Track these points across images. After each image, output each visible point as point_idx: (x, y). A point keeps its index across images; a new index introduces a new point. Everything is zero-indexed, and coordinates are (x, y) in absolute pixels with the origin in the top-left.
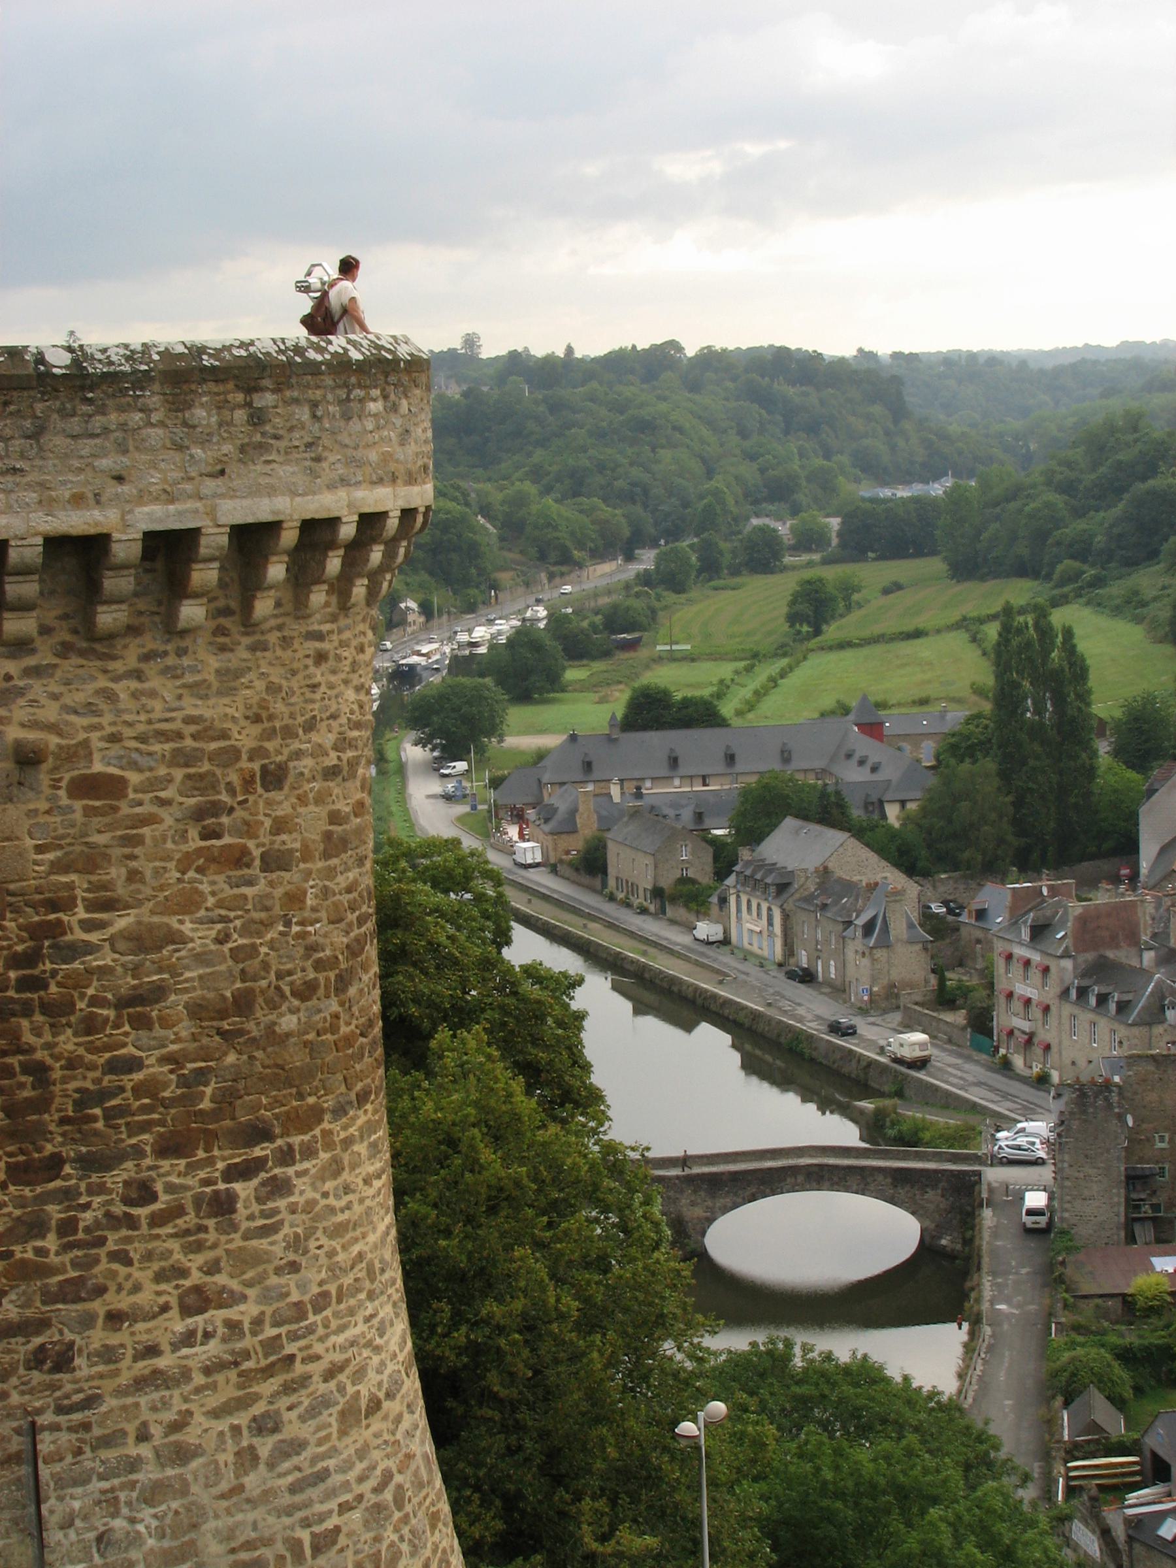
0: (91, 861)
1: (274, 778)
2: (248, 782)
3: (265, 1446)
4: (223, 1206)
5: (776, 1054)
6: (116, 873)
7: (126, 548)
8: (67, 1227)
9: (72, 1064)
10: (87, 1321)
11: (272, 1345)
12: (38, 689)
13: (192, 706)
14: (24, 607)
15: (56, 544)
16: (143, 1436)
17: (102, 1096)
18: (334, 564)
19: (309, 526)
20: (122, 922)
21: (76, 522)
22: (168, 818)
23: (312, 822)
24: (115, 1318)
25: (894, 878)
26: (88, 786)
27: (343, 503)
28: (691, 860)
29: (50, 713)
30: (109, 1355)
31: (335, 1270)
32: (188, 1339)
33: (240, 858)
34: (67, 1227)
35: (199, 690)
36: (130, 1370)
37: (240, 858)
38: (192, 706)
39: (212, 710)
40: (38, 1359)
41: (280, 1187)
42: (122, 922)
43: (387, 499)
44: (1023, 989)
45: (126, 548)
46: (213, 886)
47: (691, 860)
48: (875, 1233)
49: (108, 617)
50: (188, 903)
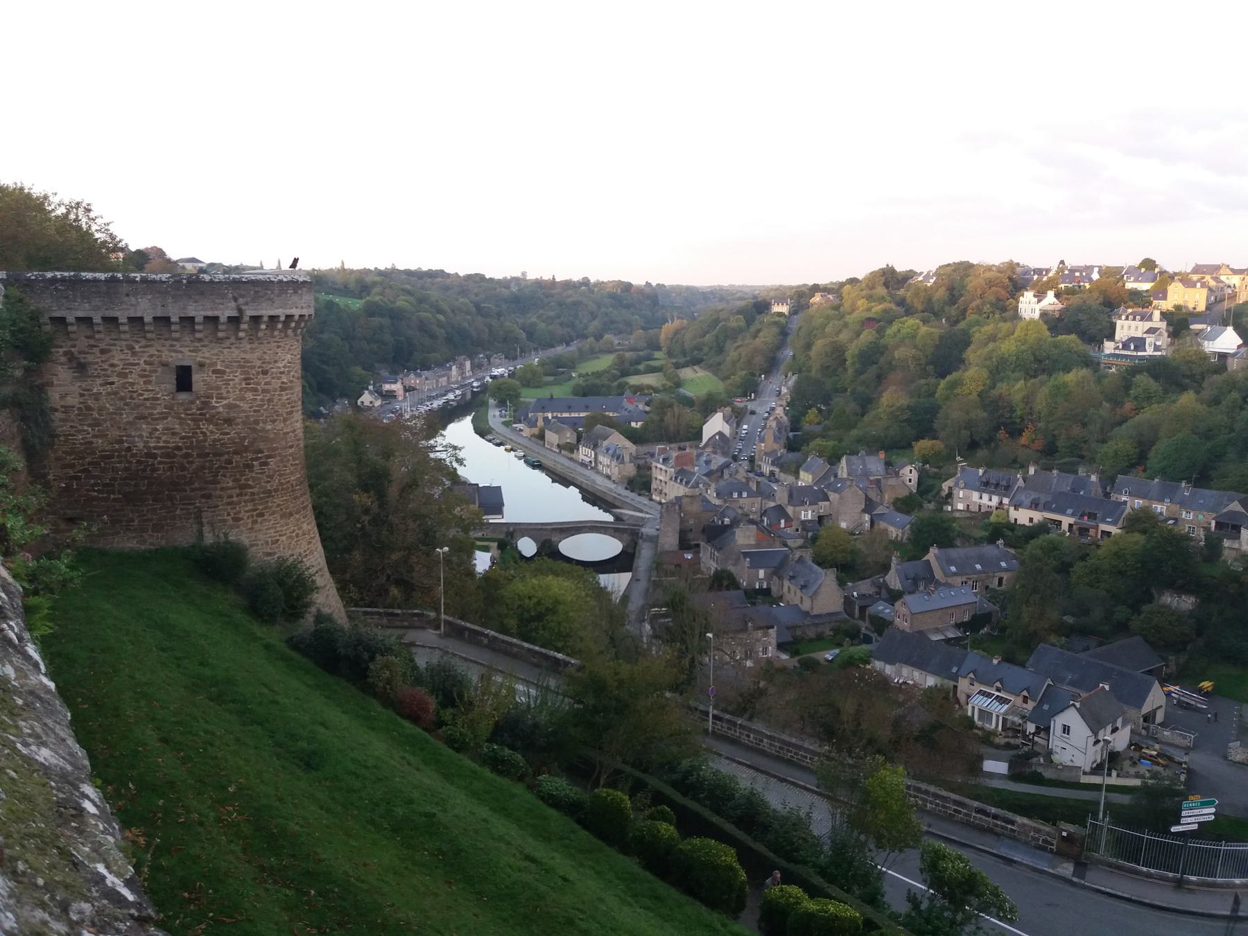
0: (218, 388)
1: (265, 373)
2: (258, 373)
3: (260, 520)
4: (249, 467)
5: (591, 497)
6: (224, 391)
7: (223, 319)
8: (210, 468)
9: (212, 432)
10: (215, 489)
11: (261, 499)
12: (204, 349)
13: (243, 355)
14: (200, 331)
15: (206, 318)
16: (229, 515)
17: (219, 440)
18: (293, 325)
19: (287, 316)
20: (225, 402)
21: (210, 313)
22: (237, 380)
23: (276, 384)
24: (222, 489)
25: (628, 444)
26: (215, 372)
27: (296, 312)
28: (569, 437)
29: (207, 355)
30: (220, 497)
31: (282, 484)
32: (240, 495)
33: (256, 390)
34: (210, 468)
35: (245, 352)
36: (225, 500)
37: (256, 390)
38: (243, 355)
39: (247, 356)
40: (203, 496)
41: (266, 464)
42: (225, 402)
43: (305, 312)
44: (660, 477)
45: (223, 319)
46: (249, 395)
47: (569, 437)
48: (609, 547)
49: (220, 335)
50: (243, 399)
